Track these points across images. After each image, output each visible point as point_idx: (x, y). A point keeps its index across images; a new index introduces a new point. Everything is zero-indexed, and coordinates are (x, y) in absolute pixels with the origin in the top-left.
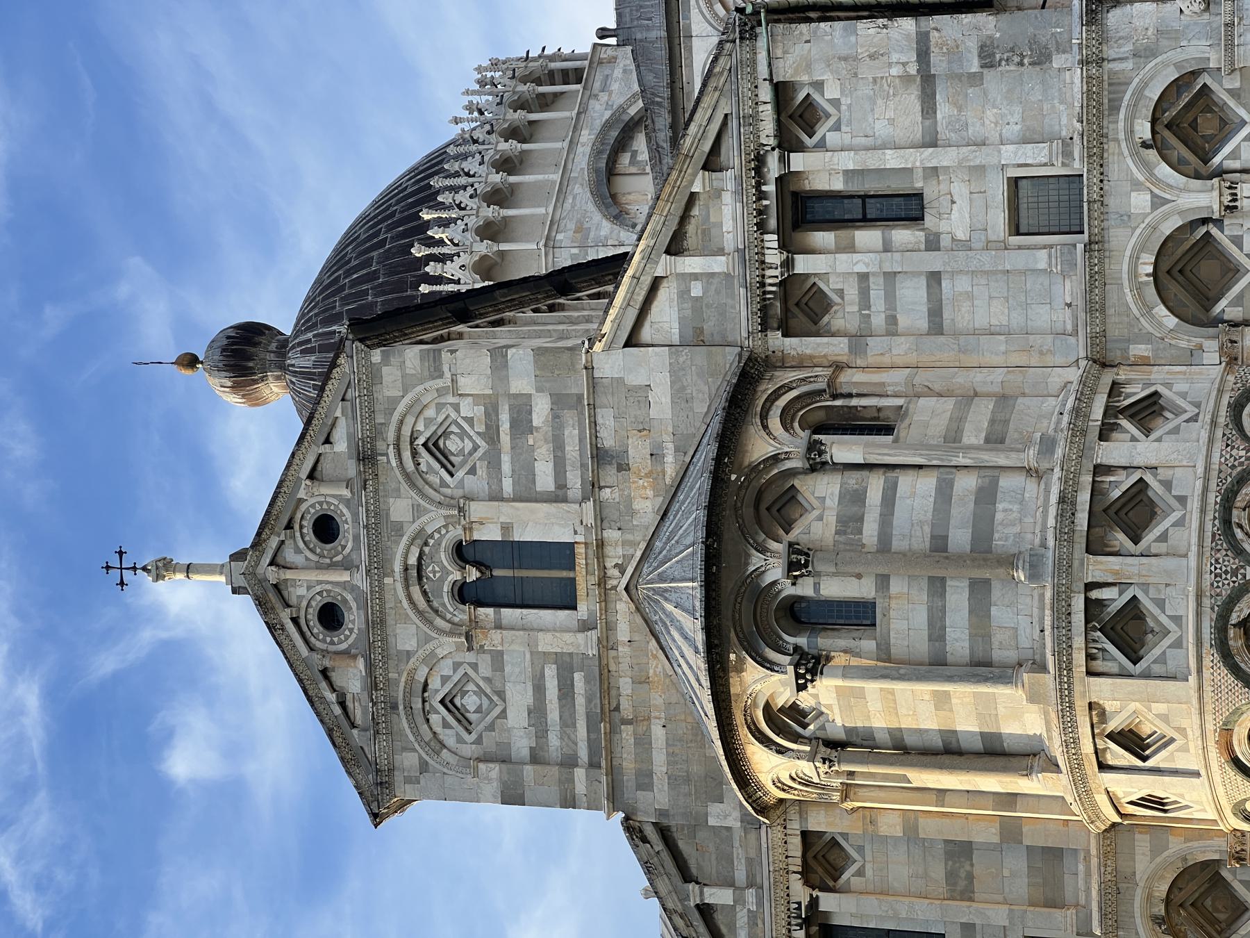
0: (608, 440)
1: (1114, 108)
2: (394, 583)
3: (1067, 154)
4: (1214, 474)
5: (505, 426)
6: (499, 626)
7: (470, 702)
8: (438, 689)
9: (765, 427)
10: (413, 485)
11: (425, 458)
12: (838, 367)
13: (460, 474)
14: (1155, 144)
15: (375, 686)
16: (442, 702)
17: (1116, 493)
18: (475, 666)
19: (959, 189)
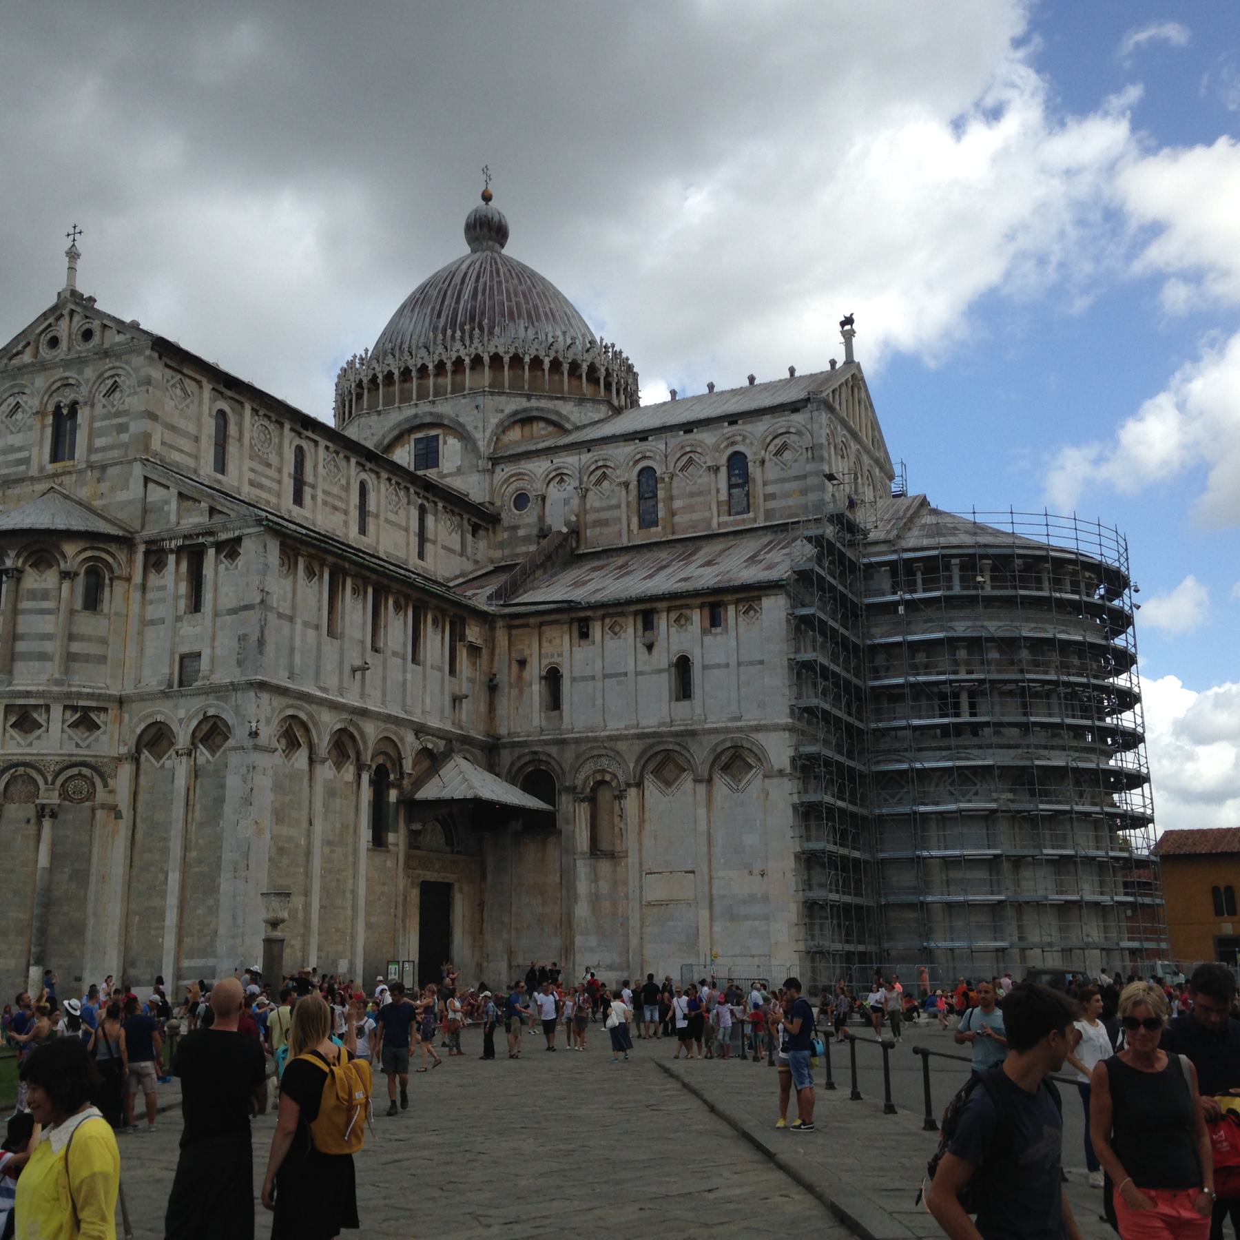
0: (112, 471)
1: (218, 699)
2: (59, 373)
3: (204, 678)
4: (41, 758)
5: (119, 420)
6: (43, 427)
7: (19, 416)
8: (21, 399)
9: (85, 550)
10: (98, 378)
11: (110, 382)
12: (128, 579)
13: (103, 401)
14: (206, 718)
15: (19, 369)
16: (18, 403)
17: (35, 715)
18: (30, 417)
19: (198, 629)
